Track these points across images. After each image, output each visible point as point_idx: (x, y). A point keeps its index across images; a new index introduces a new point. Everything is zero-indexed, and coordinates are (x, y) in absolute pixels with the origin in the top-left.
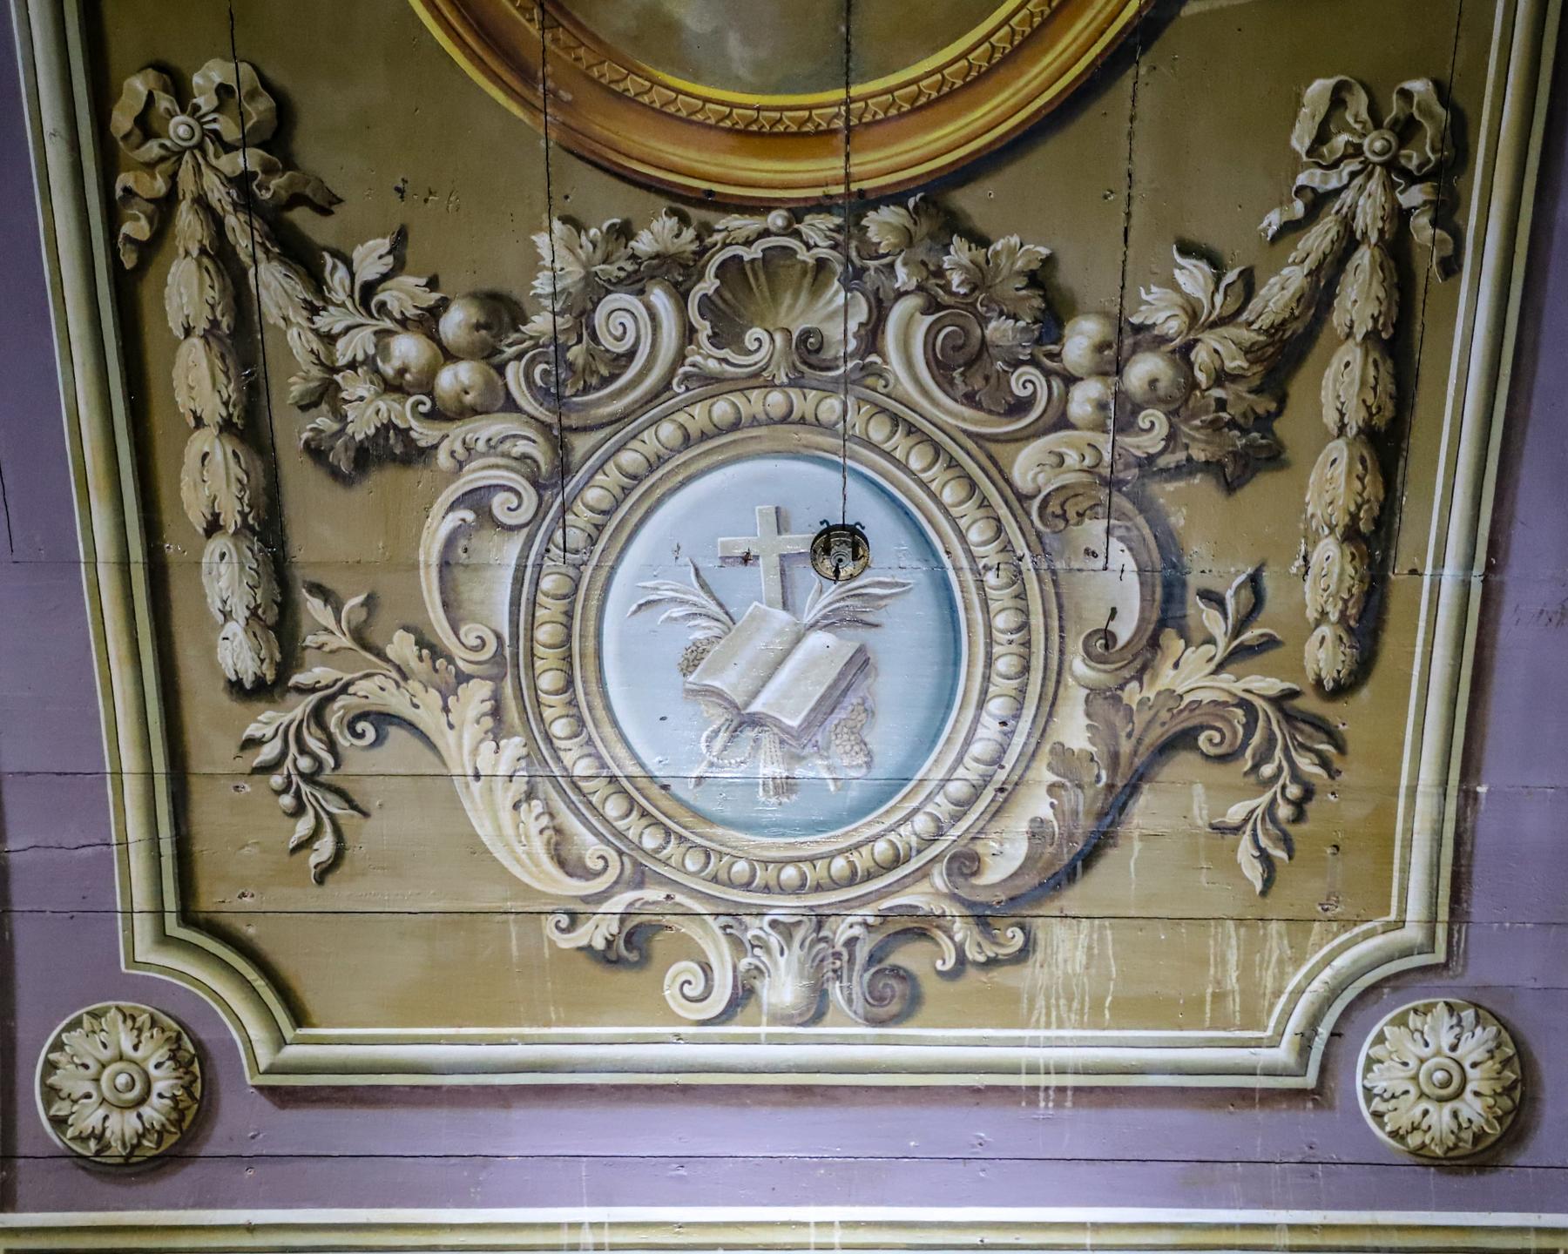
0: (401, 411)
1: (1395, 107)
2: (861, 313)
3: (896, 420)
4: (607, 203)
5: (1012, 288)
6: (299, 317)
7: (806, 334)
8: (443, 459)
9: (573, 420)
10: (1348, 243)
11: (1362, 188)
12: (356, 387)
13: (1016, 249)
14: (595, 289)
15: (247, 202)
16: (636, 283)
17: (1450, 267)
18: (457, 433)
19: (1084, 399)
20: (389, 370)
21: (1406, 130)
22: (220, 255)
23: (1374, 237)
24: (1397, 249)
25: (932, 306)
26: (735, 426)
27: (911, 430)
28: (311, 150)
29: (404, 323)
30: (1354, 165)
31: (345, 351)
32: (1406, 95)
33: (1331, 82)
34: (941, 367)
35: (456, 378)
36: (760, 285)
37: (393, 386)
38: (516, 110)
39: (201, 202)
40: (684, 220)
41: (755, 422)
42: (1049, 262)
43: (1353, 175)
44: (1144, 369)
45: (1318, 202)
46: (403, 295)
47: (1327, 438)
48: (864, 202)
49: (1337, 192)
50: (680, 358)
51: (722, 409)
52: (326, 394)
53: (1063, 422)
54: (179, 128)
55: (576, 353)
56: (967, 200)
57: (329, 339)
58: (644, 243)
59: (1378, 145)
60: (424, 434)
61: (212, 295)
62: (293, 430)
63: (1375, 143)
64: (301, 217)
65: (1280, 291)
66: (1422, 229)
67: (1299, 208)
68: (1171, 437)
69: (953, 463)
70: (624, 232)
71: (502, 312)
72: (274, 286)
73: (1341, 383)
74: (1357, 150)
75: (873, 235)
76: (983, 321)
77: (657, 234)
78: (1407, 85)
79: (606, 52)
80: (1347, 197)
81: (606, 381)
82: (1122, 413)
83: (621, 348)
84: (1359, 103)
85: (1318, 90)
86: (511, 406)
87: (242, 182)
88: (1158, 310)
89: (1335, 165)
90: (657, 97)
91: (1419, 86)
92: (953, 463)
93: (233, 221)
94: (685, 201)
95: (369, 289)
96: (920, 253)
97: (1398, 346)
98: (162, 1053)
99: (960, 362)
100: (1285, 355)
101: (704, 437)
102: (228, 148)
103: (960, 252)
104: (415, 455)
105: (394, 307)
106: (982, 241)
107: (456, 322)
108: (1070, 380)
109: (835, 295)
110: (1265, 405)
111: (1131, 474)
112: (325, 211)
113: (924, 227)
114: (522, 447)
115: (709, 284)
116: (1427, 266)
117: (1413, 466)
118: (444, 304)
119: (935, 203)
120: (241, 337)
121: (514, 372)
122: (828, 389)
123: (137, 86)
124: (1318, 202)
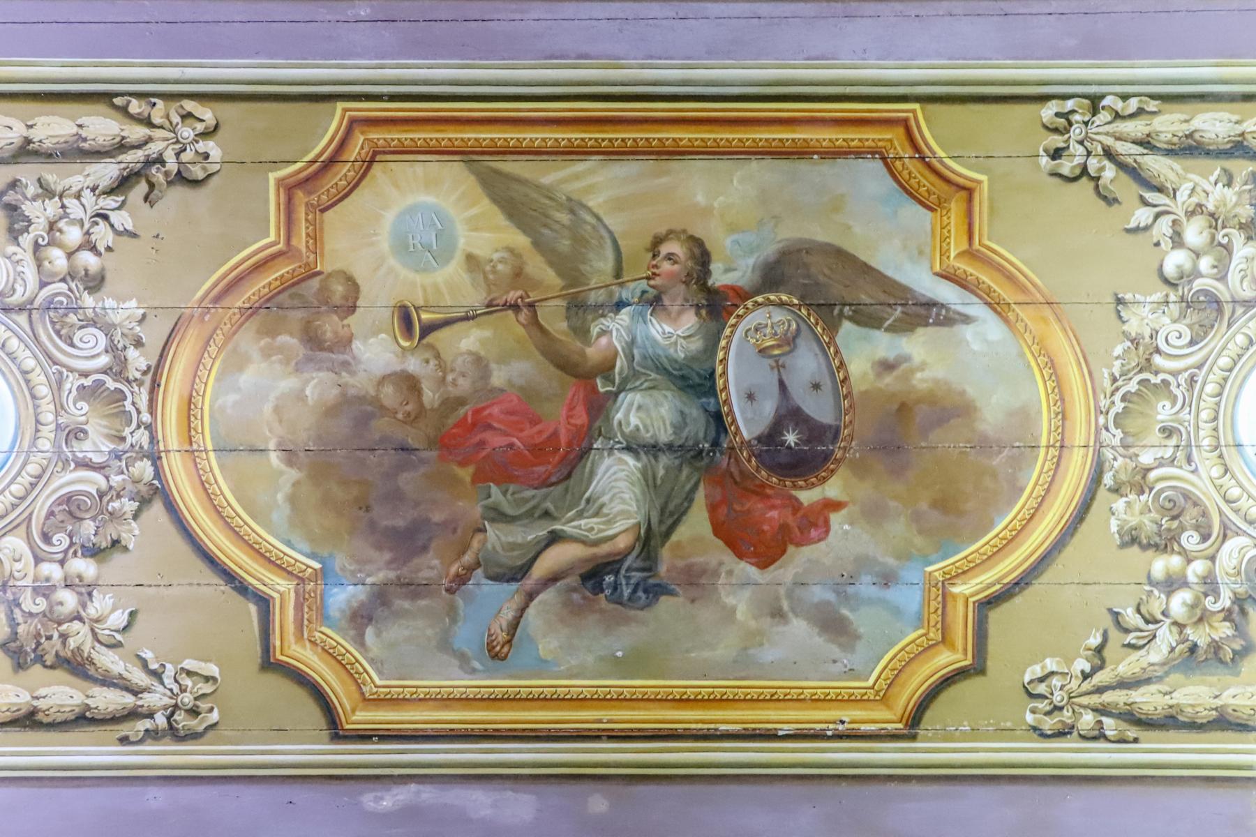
0: (38, 229)
1: (204, 706)
2: (97, 459)
3: (39, 477)
4: (154, 335)
5: (111, 532)
6: (90, 182)
7: (85, 432)
8: (12, 249)
9: (35, 315)
10: (136, 692)
11: (165, 695)
12: (52, 208)
13: (131, 533)
14: (108, 329)
15: (149, 162)
16: (111, 348)
18: (28, 258)
19: (52, 570)
20: (61, 224)
21: (194, 712)
22: (122, 146)
23: (140, 703)
24: (133, 714)
25: (101, 495)
26: (34, 397)
27: (33, 485)
28: (179, 193)
29: (88, 233)
30: (176, 690)
31: (71, 203)
32: (211, 710)
33: (217, 675)
34: (68, 499)
35: (57, 257)
36: (112, 409)
37: (52, 226)
38: (200, 293)
39: (149, 140)
40: (145, 373)
41: (36, 407)
42: (126, 549)
43: (171, 690)
44: (69, 600)
45: (157, 675)
46: (102, 235)
47: (31, 691)
48: (155, 459)
49: (162, 683)
50: (71, 370)
51: (43, 390)
52: (47, 192)
53: (38, 560)
54: (187, 132)
55: (72, 318)
56: (157, 507)
57: (78, 196)
58: (132, 353)
59: (186, 700)
60: (26, 240)
61: (101, 140)
62: (27, 174)
64: (142, 187)
65: (110, 661)
67: (154, 666)
68: (31, 614)
69: (14, 506)
70: (138, 343)
71: (95, 283)
72: (107, 172)
73: (62, 695)
74: (183, 691)
75: (138, 464)
76: (94, 519)
77: (137, 360)
78: (216, 710)
79: (228, 338)
80: (160, 688)
81: (58, 333)
82: (44, 590)
83: (76, 340)
84: (207, 688)
85: (213, 670)
86: (43, 285)
87: (160, 160)
88: (100, 604)
89: (176, 681)
90: (207, 361)
93: (139, 155)
94: (155, 375)
95: (105, 217)
96: (129, 487)
99: (71, 508)
100: (77, 666)
101: (27, 381)
102: (178, 155)
103: (130, 506)
104: (14, 235)
105: (95, 229)
106: (136, 516)
107: (88, 260)
108: (62, 563)
109: (107, 446)
110: (49, 659)
111: (9, 596)
112: (146, 199)
113: (143, 489)
114: (19, 290)
115: (111, 384)
116: (125, 729)
118: (99, 254)
119: (157, 493)
120: (79, 152)
121: (62, 287)
122: (55, 443)
123: (207, 114)
124: (157, 675)
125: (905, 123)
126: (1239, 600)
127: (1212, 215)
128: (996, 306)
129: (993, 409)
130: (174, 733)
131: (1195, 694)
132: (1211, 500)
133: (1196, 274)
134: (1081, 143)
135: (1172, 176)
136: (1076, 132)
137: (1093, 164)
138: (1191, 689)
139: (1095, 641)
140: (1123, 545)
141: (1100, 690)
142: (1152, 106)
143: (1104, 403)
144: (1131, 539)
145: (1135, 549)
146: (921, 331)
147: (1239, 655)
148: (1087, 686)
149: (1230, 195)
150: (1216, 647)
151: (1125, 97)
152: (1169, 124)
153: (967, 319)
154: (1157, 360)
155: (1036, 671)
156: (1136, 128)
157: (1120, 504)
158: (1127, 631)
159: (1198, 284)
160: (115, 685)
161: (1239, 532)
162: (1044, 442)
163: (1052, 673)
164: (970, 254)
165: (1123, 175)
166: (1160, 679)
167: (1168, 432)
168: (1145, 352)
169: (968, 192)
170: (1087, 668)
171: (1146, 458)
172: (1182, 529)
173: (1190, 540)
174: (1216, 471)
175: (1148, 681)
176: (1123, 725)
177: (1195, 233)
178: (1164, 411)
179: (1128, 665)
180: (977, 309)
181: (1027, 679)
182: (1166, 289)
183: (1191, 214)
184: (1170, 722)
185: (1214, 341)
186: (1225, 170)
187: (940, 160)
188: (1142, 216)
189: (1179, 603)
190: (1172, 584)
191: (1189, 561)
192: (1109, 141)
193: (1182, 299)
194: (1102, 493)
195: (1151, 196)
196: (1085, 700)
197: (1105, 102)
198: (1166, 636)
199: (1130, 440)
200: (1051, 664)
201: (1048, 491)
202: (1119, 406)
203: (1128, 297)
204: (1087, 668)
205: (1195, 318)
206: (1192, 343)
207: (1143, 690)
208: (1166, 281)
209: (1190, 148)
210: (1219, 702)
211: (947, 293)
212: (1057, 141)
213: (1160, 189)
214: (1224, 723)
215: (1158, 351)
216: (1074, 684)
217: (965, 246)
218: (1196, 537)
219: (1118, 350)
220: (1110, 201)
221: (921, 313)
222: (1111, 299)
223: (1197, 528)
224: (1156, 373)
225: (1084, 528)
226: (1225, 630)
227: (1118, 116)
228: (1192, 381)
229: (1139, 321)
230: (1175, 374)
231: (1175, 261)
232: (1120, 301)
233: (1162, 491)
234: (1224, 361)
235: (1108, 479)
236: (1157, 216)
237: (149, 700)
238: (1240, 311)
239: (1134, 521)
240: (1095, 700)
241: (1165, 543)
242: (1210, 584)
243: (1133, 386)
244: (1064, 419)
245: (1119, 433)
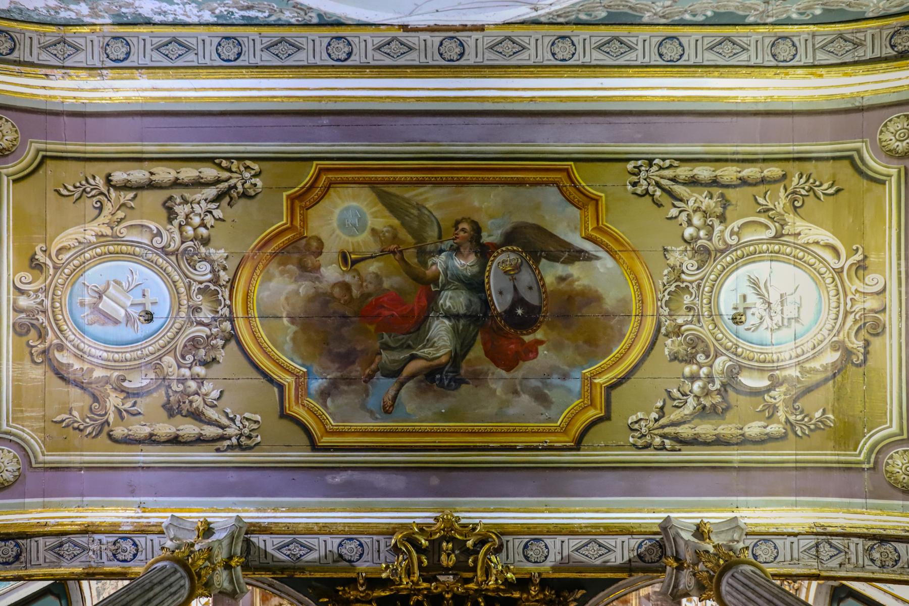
0: (181, 218)
1: (254, 434)
2: (206, 321)
3: (180, 329)
4: (232, 265)
5: (212, 354)
6: (204, 197)
7: (201, 309)
8: (169, 227)
9: (179, 256)
10: (223, 427)
12: (187, 208)
13: (221, 355)
14: (211, 262)
15: (231, 188)
16: (213, 271)
17: (218, 450)
18: (176, 231)
19: (186, 372)
20: (191, 216)
21: (249, 437)
22: (218, 181)
24: (222, 438)
25: (208, 337)
26: (178, 293)
27: (177, 333)
28: (243, 202)
29: (203, 220)
31: (196, 206)
34: (193, 339)
35: (189, 231)
36: (213, 298)
37: (187, 216)
38: (252, 246)
39: (230, 178)
40: (227, 282)
41: (179, 298)
42: (218, 362)
44: (193, 385)
45: (233, 420)
46: (209, 220)
47: (176, 427)
48: (231, 320)
50: (195, 281)
51: (182, 290)
52: (185, 201)
53: (179, 367)
54: (247, 175)
55: (196, 257)
56: (233, 344)
57: (199, 203)
58: (222, 273)
60: (176, 223)
61: (209, 178)
62: (176, 193)
63: (246, 431)
64: (227, 199)
65: (212, 413)
66: (228, 443)
68: (176, 392)
70: (225, 269)
71: (206, 242)
72: (212, 192)
73: (190, 429)
74: (244, 427)
75: (224, 323)
76: (204, 348)
77: (224, 276)
79: (265, 266)
81: (189, 264)
82: (182, 380)
83: (197, 267)
84: (255, 426)
85: (258, 418)
86: (183, 242)
87: (235, 187)
88: (207, 387)
90: (255, 276)
91: (259, 439)
92: (169, 342)
93: (226, 185)
94: (232, 282)
95: (211, 212)
96: (220, 334)
97: (200, 440)
98: (5, 146)
99: (194, 343)
100: (197, 416)
101: (175, 286)
102: (243, 185)
103: (220, 342)
104: (170, 221)
105: (206, 218)
106: (223, 347)
107: (203, 231)
108: (190, 368)
109: (210, 315)
110: (184, 413)
111: (166, 383)
112: (229, 204)
113: (227, 335)
114: (172, 245)
115: (212, 287)
116: (218, 445)
117: (169, 447)
118: (207, 229)
119: (232, 337)
120: (199, 184)
121: (191, 243)
122: (187, 314)
123: (256, 167)
124: (233, 420)
125: (567, 170)
126: (724, 385)
127: (704, 212)
128: (610, 252)
129: (610, 300)
130: (240, 447)
131: (705, 429)
132: (710, 340)
133: (698, 238)
134: (645, 179)
135: (686, 194)
136: (643, 175)
137: (651, 189)
138: (703, 426)
139: (660, 404)
140: (671, 360)
141: (663, 427)
142: (676, 163)
143: (660, 296)
144: (675, 358)
145: (677, 362)
146: (577, 263)
147: (725, 410)
148: (656, 425)
149: (712, 203)
150: (714, 406)
151: (664, 160)
152: (683, 172)
153: (597, 258)
154: (683, 276)
155: (633, 418)
156: (669, 173)
157: (669, 342)
158: (674, 400)
159: (700, 242)
160: (214, 425)
161: (722, 354)
162: (634, 314)
163: (641, 419)
164: (598, 229)
165: (665, 195)
166: (689, 422)
167: (689, 309)
168: (677, 273)
169: (596, 201)
170: (657, 416)
171: (680, 321)
172: (697, 353)
173: (701, 358)
174: (711, 327)
175: (684, 423)
176: (674, 443)
177: (697, 220)
178: (687, 299)
179: (675, 416)
180: (602, 254)
181: (630, 422)
182: (686, 245)
183: (695, 211)
184: (694, 442)
185: (707, 268)
186: (709, 192)
187: (583, 187)
188: (674, 212)
189: (697, 386)
190: (693, 378)
191: (701, 368)
192: (658, 179)
193: (693, 249)
194: (661, 337)
195: (677, 203)
196: (656, 432)
197: (655, 162)
198: (691, 402)
199: (672, 313)
200: (640, 415)
201: (636, 336)
202: (667, 297)
203: (669, 248)
204: (657, 416)
205: (699, 258)
206: (698, 269)
207: (682, 427)
208: (685, 241)
209: (693, 182)
210: (716, 432)
211: (588, 246)
212: (635, 179)
213: (681, 200)
214: (719, 442)
215: (683, 272)
216: (651, 424)
217: (595, 225)
218: (703, 357)
219: (666, 272)
220: (659, 205)
221: (577, 255)
222: (661, 249)
223: (704, 352)
224: (683, 282)
225: (653, 352)
226: (718, 399)
227: (661, 168)
228: (699, 286)
229: (675, 258)
230: (691, 282)
231: (689, 232)
232: (665, 250)
233: (687, 336)
234: (712, 277)
235: (663, 330)
236: (680, 212)
237: (229, 431)
238: (719, 254)
239: (676, 349)
240: (660, 431)
241: (690, 359)
242: (710, 378)
243: (673, 288)
244: (642, 303)
245: (667, 309)
